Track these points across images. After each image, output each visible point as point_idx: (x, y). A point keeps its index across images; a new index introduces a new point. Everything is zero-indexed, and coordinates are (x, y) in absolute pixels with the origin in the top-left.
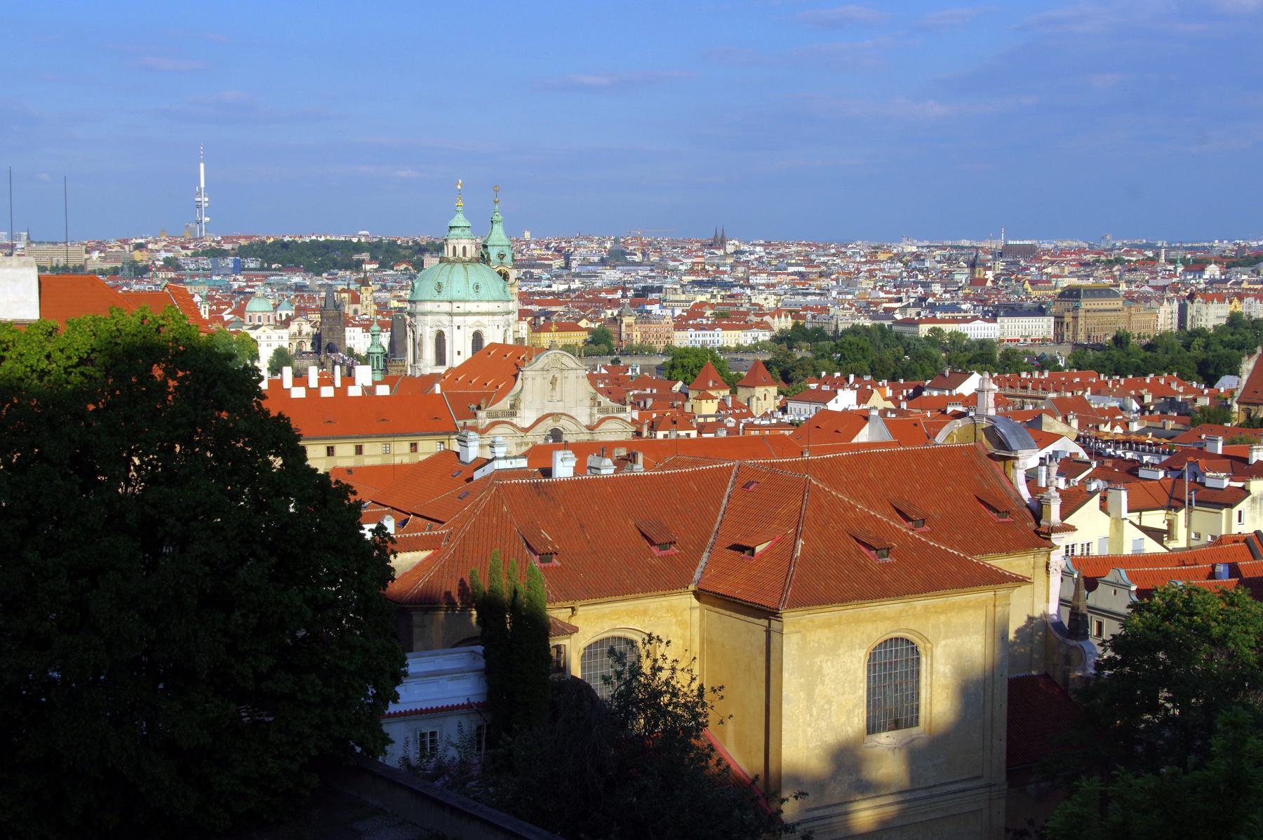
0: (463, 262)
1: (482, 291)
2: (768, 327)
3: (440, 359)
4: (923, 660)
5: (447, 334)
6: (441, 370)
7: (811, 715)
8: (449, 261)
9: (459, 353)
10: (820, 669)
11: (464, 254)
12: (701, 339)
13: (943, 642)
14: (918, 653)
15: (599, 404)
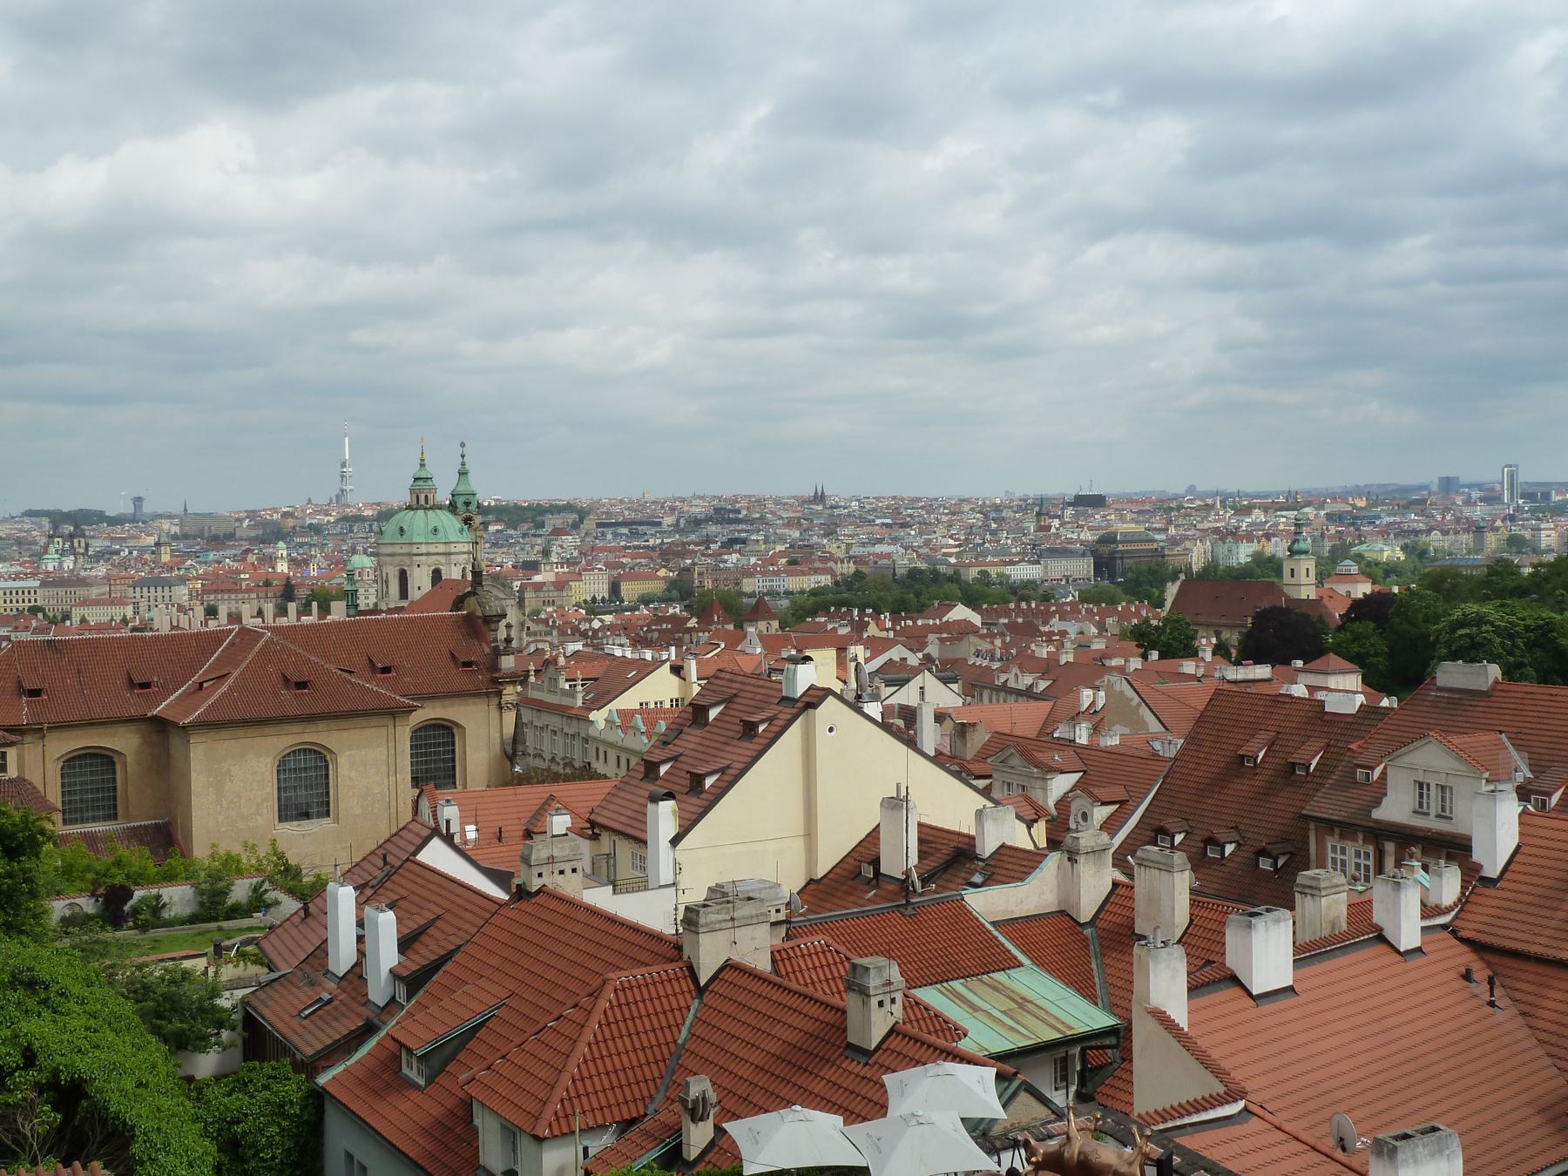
0: (425, 509)
1: (441, 537)
2: (831, 572)
3: (404, 594)
4: (331, 767)
5: (408, 572)
6: (404, 604)
7: (222, 807)
8: (413, 509)
9: (419, 588)
10: (229, 771)
11: (427, 502)
12: (768, 584)
13: (348, 753)
14: (326, 761)
15: (528, 628)
